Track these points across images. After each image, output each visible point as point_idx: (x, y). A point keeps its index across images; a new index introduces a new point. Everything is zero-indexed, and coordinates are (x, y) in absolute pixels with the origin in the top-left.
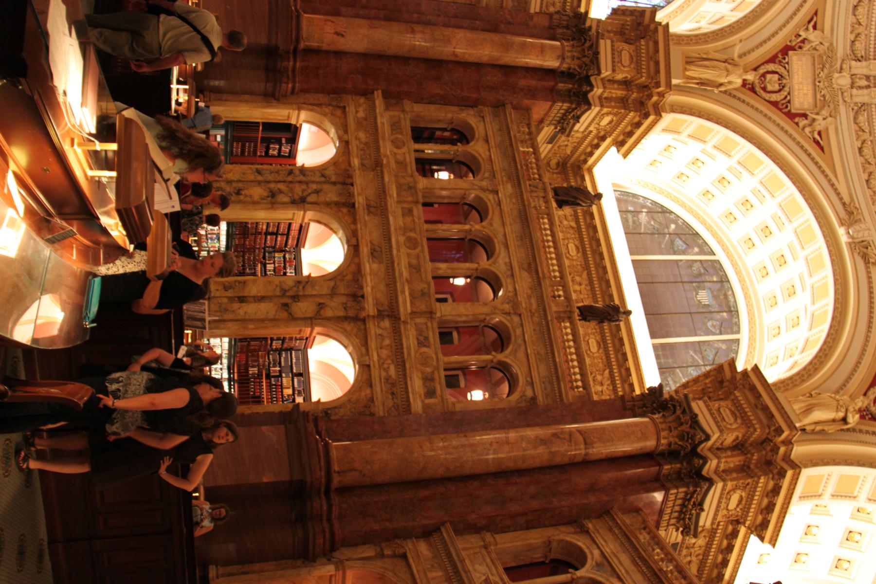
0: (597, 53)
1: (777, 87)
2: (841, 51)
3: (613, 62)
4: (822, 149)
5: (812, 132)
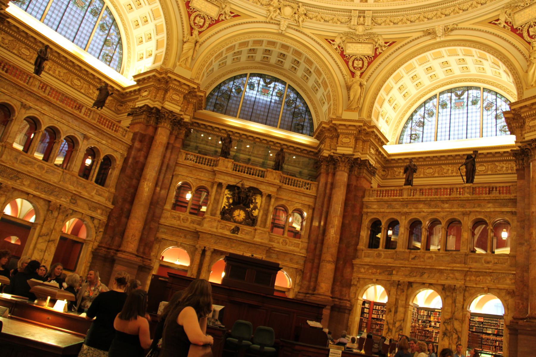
0: (171, 112)
1: (203, 20)
3: (176, 105)
4: (238, 16)
5: (230, 16)
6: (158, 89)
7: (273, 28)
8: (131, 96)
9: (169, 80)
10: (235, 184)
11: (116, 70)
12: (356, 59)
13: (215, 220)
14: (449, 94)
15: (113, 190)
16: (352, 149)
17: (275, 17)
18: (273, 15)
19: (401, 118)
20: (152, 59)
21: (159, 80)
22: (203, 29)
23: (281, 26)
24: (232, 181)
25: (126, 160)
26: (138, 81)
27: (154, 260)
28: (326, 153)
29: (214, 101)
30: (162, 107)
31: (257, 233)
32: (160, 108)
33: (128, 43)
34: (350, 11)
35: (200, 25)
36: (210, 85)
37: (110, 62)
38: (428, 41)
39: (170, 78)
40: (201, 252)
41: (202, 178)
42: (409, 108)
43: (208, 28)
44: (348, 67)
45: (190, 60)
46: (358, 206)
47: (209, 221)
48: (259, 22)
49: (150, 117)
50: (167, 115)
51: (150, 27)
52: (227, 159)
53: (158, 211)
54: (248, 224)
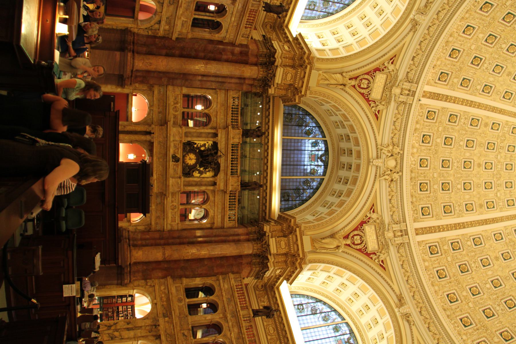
0: (274, 76)
1: (366, 87)
2: (401, 75)
4: (377, 118)
6: (293, 59)
7: (373, 153)
8: (282, 34)
9: (304, 67)
10: (219, 149)
11: (303, 16)
12: (361, 237)
13: (181, 138)
14: (348, 332)
15: (190, 36)
16: (275, 252)
17: (384, 153)
18: (385, 150)
19: (315, 292)
20: (321, 47)
21: (302, 58)
22: (358, 88)
23: (377, 160)
24: (221, 146)
25: (220, 42)
26: (296, 39)
27: (131, 88)
28: (266, 228)
29: (294, 112)
30: (277, 66)
31: (177, 179)
32: (276, 64)
33: (330, 22)
34: (404, 221)
35: (360, 85)
36: (308, 105)
37: (309, 9)
38: (393, 300)
39: (306, 67)
40: (148, 130)
41: (218, 117)
42: (327, 297)
43: (360, 93)
44: (352, 231)
45: (327, 82)
46: (223, 270)
47: (179, 133)
48: (376, 139)
49: (266, 57)
50: (270, 72)
51: (349, 40)
52: (241, 136)
53: (179, 82)
54: (184, 169)
